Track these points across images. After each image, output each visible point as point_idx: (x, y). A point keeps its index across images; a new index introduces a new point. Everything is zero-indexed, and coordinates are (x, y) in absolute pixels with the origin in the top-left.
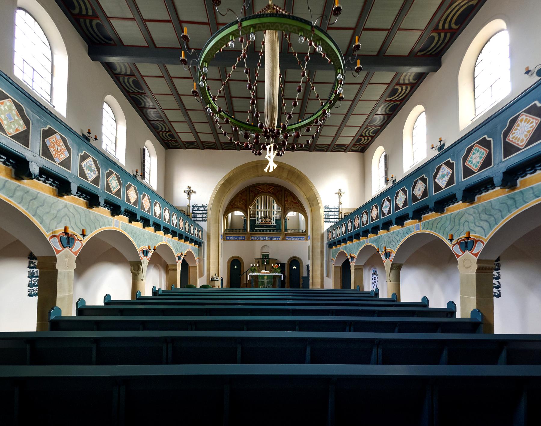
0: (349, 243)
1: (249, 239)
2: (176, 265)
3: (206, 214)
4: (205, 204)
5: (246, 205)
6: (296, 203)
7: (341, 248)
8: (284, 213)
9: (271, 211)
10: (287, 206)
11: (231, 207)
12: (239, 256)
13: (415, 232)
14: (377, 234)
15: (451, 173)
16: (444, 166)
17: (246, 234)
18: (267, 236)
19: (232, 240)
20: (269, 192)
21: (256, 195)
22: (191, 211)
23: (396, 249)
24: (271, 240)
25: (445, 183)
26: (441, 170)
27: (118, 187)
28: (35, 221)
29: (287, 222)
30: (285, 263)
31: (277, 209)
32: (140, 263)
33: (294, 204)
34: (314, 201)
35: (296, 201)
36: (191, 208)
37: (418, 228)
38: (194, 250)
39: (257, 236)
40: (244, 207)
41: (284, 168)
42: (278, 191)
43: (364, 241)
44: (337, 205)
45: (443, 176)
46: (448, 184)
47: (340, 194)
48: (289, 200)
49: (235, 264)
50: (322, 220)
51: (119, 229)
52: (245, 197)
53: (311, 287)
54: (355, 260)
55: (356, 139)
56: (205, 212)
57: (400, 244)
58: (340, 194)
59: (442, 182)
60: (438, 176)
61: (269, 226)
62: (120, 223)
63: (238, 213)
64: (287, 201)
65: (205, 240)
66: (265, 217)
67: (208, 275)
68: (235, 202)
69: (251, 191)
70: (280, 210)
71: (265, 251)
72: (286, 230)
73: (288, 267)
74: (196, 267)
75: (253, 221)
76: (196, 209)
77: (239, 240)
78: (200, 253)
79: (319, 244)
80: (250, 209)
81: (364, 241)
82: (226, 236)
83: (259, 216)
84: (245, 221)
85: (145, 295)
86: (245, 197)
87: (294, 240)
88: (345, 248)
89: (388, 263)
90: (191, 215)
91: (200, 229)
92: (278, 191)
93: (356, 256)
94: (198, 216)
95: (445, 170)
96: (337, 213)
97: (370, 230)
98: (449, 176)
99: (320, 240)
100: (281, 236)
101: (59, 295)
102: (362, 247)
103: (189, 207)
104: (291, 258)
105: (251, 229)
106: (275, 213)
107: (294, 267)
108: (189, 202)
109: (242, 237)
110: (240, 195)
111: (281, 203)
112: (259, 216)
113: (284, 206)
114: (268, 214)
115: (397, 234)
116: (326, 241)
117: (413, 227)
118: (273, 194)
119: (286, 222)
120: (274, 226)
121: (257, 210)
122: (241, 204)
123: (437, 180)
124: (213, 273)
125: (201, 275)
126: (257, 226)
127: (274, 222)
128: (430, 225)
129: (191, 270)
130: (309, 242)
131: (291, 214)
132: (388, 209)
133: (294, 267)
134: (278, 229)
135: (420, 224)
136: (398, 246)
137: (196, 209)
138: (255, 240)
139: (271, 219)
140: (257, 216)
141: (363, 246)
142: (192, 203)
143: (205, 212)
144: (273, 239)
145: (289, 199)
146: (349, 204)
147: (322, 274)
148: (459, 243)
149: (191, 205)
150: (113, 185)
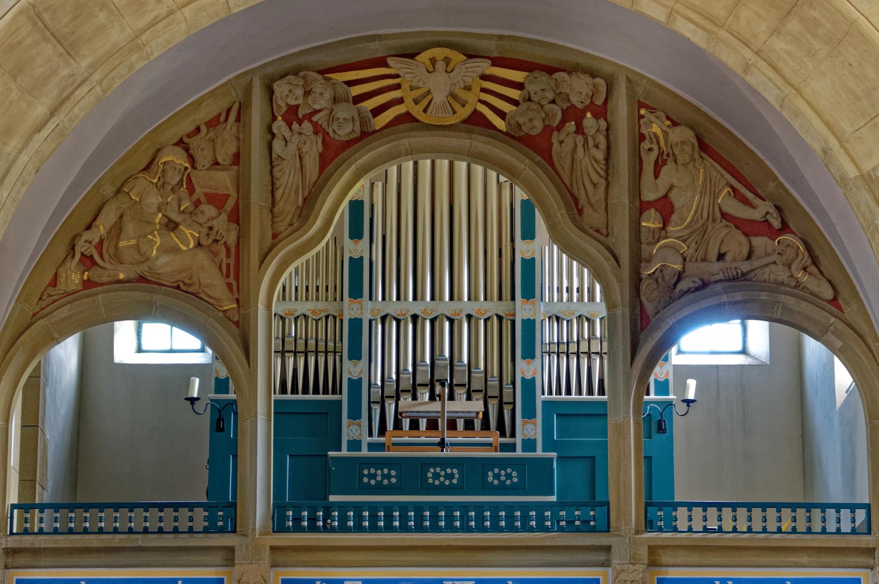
5: (237, 252)
6: (764, 228)
8: (642, 331)
11: (73, 277)
21: (333, 154)
29: (678, 425)
31: (569, 288)
33: (737, 244)
35: (760, 210)
48: (689, 204)
61: (474, 474)
64: (665, 208)
68: (117, 229)
70: (599, 308)
72: (657, 507)
75: (309, 424)
80: (285, 292)
84: (224, 418)
86: (223, 181)
92: (573, 114)
106: (549, 333)
110: (175, 158)
111: (602, 235)
113: (638, 260)
114: (471, 349)
118: (517, 138)
119: (657, 424)
120: (535, 475)
122: (176, 253)
126: (353, 475)
127: (530, 429)
131: (716, 343)
140: (351, 370)
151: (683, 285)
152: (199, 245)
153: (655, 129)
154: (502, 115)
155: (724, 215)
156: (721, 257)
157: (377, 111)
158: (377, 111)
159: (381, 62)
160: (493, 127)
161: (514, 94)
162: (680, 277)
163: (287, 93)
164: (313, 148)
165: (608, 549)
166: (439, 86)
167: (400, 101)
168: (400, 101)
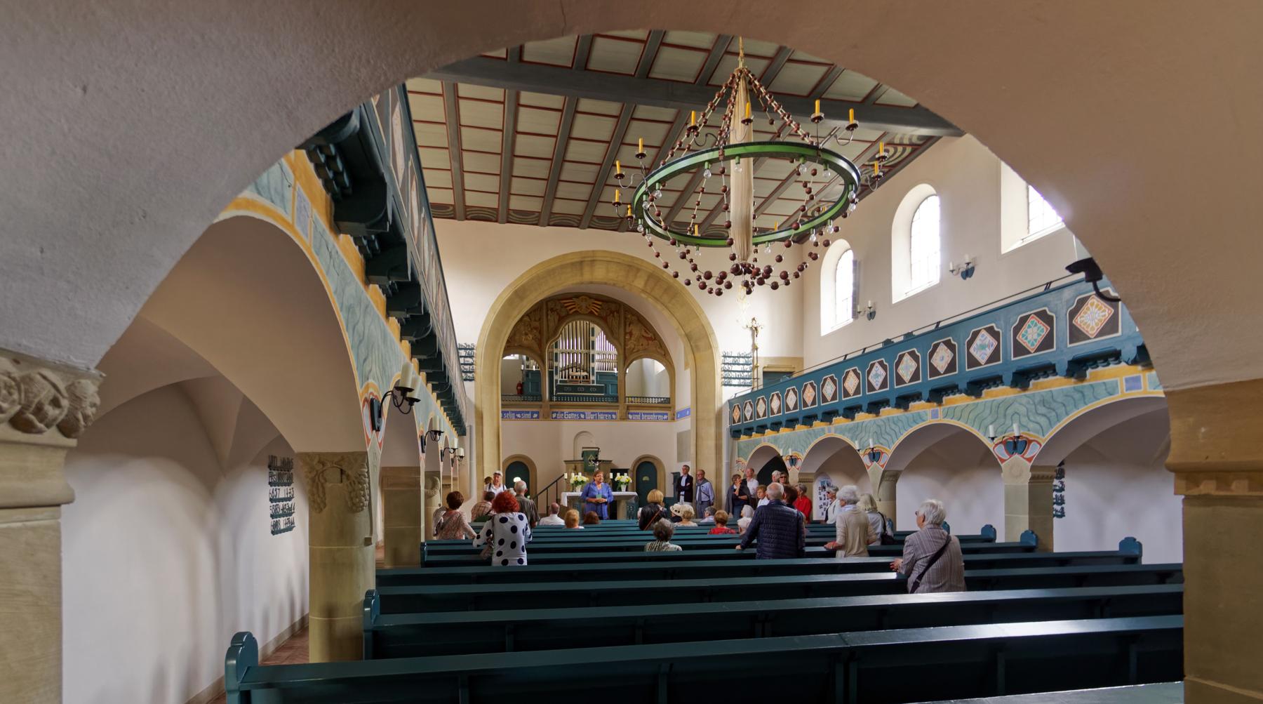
0: (784, 431)
1: (547, 417)
4: (469, 343)
7: (767, 438)
9: (587, 355)
10: (631, 345)
13: (930, 421)
14: (853, 419)
15: (995, 343)
16: (984, 332)
17: (541, 407)
18: (588, 412)
20: (591, 313)
21: (562, 320)
23: (893, 447)
24: (596, 418)
25: (986, 358)
26: (979, 337)
33: (645, 342)
34: (700, 341)
35: (650, 335)
37: (935, 415)
39: (566, 411)
40: (536, 346)
41: (638, 270)
42: (612, 312)
43: (823, 430)
44: (747, 350)
45: (983, 347)
46: (990, 360)
47: (755, 330)
50: (718, 381)
52: (537, 324)
54: (799, 463)
55: (793, 220)
56: (470, 360)
57: (902, 438)
58: (755, 330)
59: (982, 355)
60: (974, 345)
64: (631, 334)
66: (575, 366)
69: (552, 310)
71: (592, 444)
77: (526, 419)
79: (712, 431)
81: (823, 430)
83: (561, 364)
86: (537, 324)
87: (646, 420)
88: (776, 440)
89: (875, 470)
93: (802, 456)
95: (985, 339)
96: (747, 368)
97: (841, 412)
98: (992, 349)
99: (713, 422)
100: (618, 411)
102: (816, 441)
104: (640, 459)
107: (645, 478)
109: (533, 413)
110: (526, 319)
111: (618, 339)
112: (561, 364)
115: (896, 421)
116: (726, 425)
117: (924, 413)
118: (600, 317)
120: (599, 389)
123: (972, 350)
128: (958, 411)
130: (686, 424)
132: (881, 380)
134: (604, 394)
135: (940, 410)
136: (897, 442)
141: (820, 439)
143: (470, 360)
144: (601, 417)
145: (636, 331)
146: (770, 349)
148: (1005, 443)
163: (551, 305)
164: (557, 318)
166: (584, 304)
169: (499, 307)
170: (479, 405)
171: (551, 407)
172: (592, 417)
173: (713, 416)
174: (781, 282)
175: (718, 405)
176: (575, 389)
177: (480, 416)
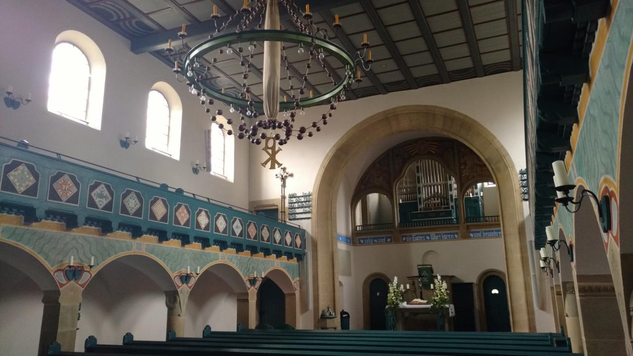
2: (247, 294)
3: (309, 207)
9: (446, 185)
12: (370, 273)
17: (391, 232)
18: (433, 234)
19: (369, 244)
22: (287, 205)
24: (440, 239)
27: (138, 206)
28: (41, 258)
30: (471, 284)
32: (176, 293)
36: (287, 201)
38: (287, 267)
39: (414, 234)
49: (376, 286)
51: (144, 252)
53: (512, 331)
62: (146, 245)
63: (373, 198)
64: (465, 164)
65: (309, 252)
67: (316, 308)
73: (479, 292)
74: (294, 294)
76: (294, 200)
77: (381, 243)
78: (302, 273)
82: (356, 238)
85: (185, 336)
90: (287, 212)
91: (302, 233)
94: (298, 211)
101: (60, 330)
103: (283, 197)
104: (485, 273)
105: (400, 223)
107: (495, 291)
108: (283, 191)
109: (387, 238)
121: (418, 185)
124: (323, 304)
125: (305, 308)
129: (287, 300)
133: (495, 291)
137: (294, 200)
138: (409, 242)
139: (448, 199)
142: (288, 191)
144: (445, 237)
147: (529, 304)
149: (287, 195)
150: (130, 205)
151: (470, 178)
152: (383, 179)
153: (462, 150)
154: (433, 150)
155: (477, 164)
156: (476, 172)
157: (412, 153)
158: (412, 153)
159: (412, 144)
160: (432, 153)
161: (436, 147)
162: (469, 176)
165: (458, 227)
167: (415, 151)
168: (415, 151)
169: (327, 162)
170: (314, 236)
171: (401, 232)
172: (436, 237)
173: (516, 230)
174: (314, 130)
175: (519, 220)
176: (437, 214)
177: (315, 245)
